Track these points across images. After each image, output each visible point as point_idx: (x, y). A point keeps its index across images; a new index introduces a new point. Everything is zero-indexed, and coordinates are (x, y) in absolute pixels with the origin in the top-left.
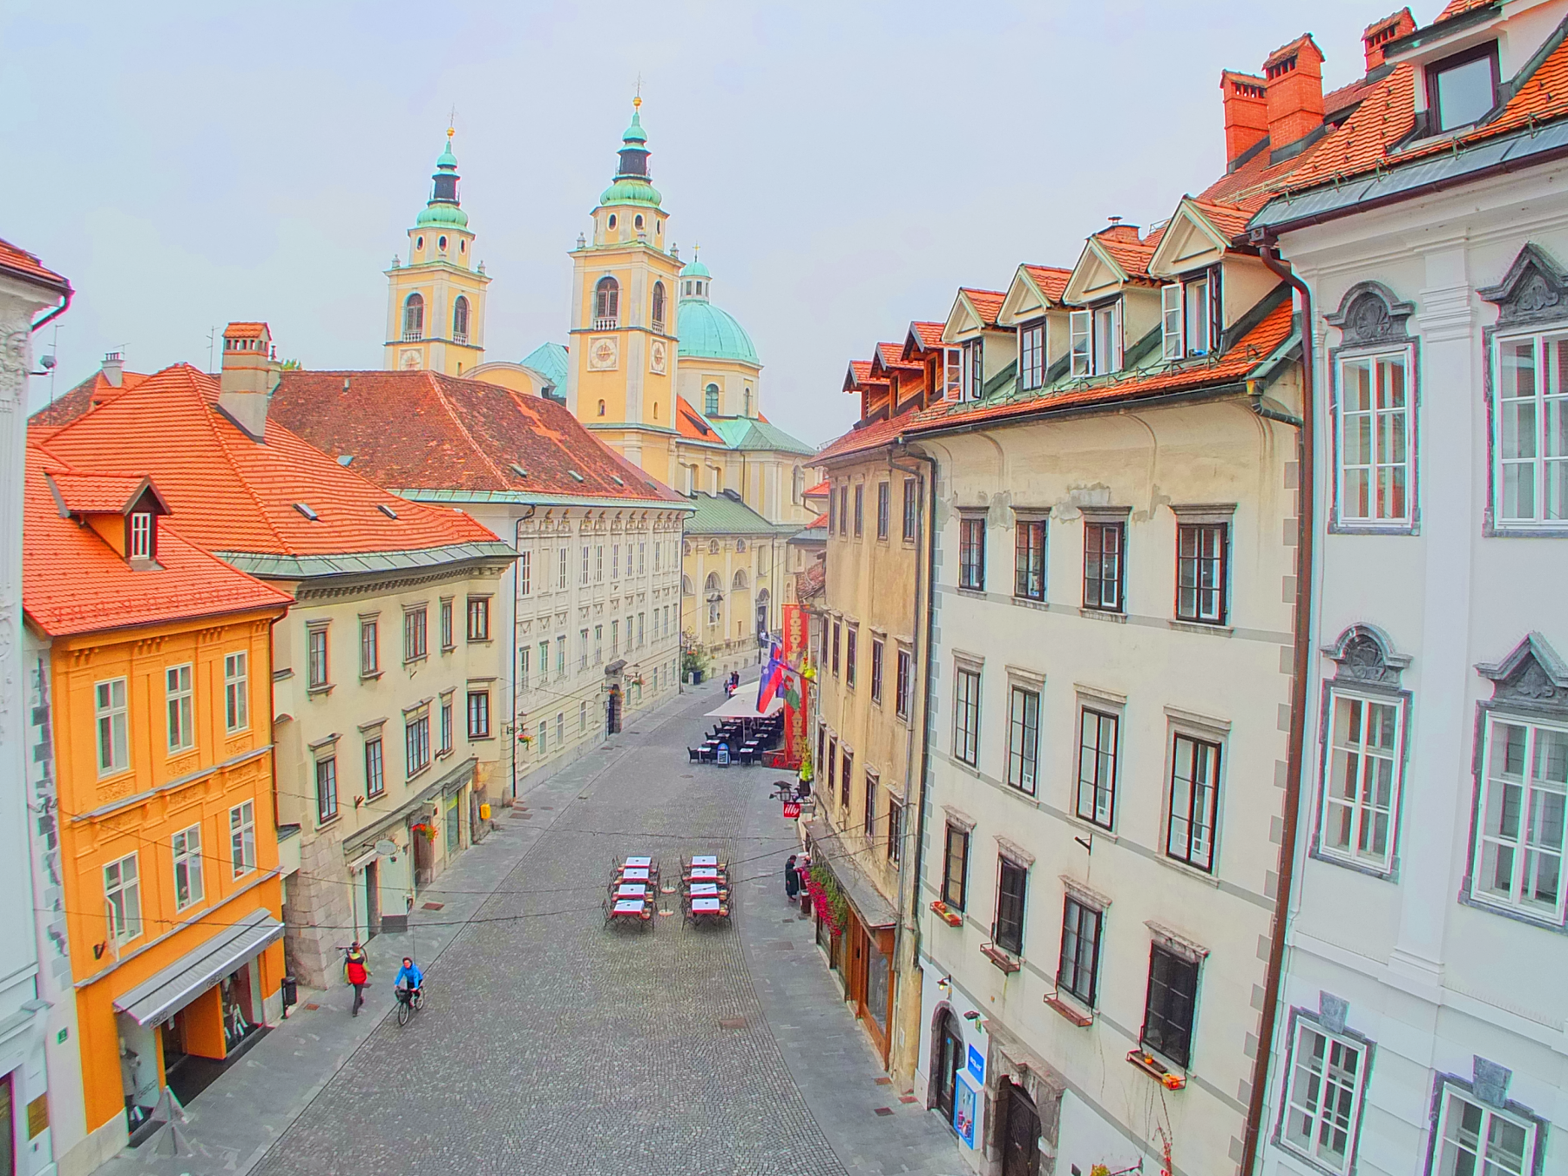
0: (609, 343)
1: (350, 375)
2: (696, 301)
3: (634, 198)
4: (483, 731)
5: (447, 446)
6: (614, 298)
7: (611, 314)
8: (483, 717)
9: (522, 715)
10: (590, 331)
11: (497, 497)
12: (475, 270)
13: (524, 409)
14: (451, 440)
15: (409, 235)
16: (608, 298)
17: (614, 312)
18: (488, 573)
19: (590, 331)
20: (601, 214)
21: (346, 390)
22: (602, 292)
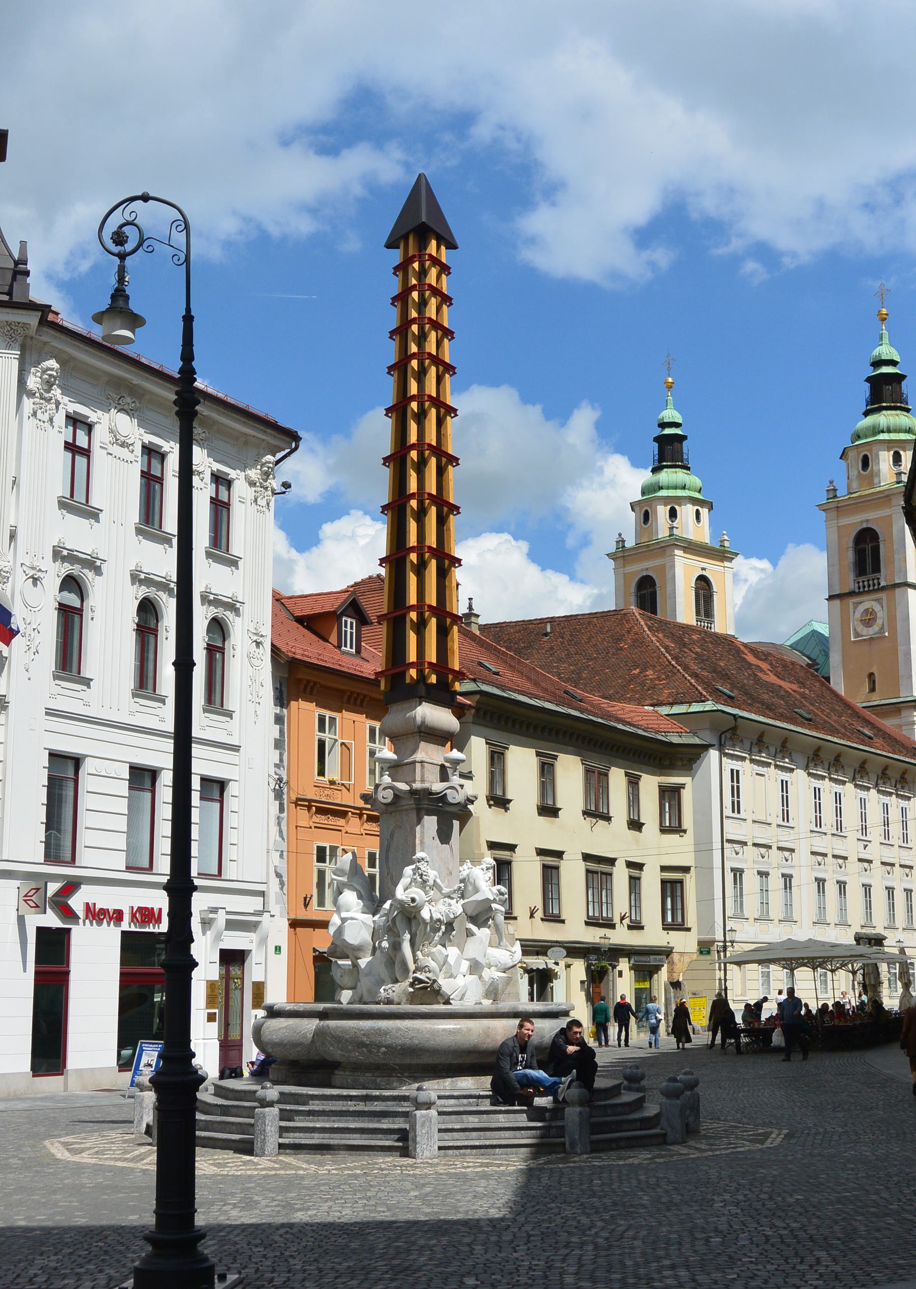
0: (877, 607)
1: (552, 620)
3: (889, 431)
5: (649, 672)
6: (876, 551)
7: (873, 572)
8: (679, 906)
9: (731, 930)
10: (852, 594)
11: (696, 707)
13: (750, 658)
14: (654, 667)
16: (869, 552)
17: (877, 568)
19: (852, 594)
20: (851, 454)
21: (546, 634)
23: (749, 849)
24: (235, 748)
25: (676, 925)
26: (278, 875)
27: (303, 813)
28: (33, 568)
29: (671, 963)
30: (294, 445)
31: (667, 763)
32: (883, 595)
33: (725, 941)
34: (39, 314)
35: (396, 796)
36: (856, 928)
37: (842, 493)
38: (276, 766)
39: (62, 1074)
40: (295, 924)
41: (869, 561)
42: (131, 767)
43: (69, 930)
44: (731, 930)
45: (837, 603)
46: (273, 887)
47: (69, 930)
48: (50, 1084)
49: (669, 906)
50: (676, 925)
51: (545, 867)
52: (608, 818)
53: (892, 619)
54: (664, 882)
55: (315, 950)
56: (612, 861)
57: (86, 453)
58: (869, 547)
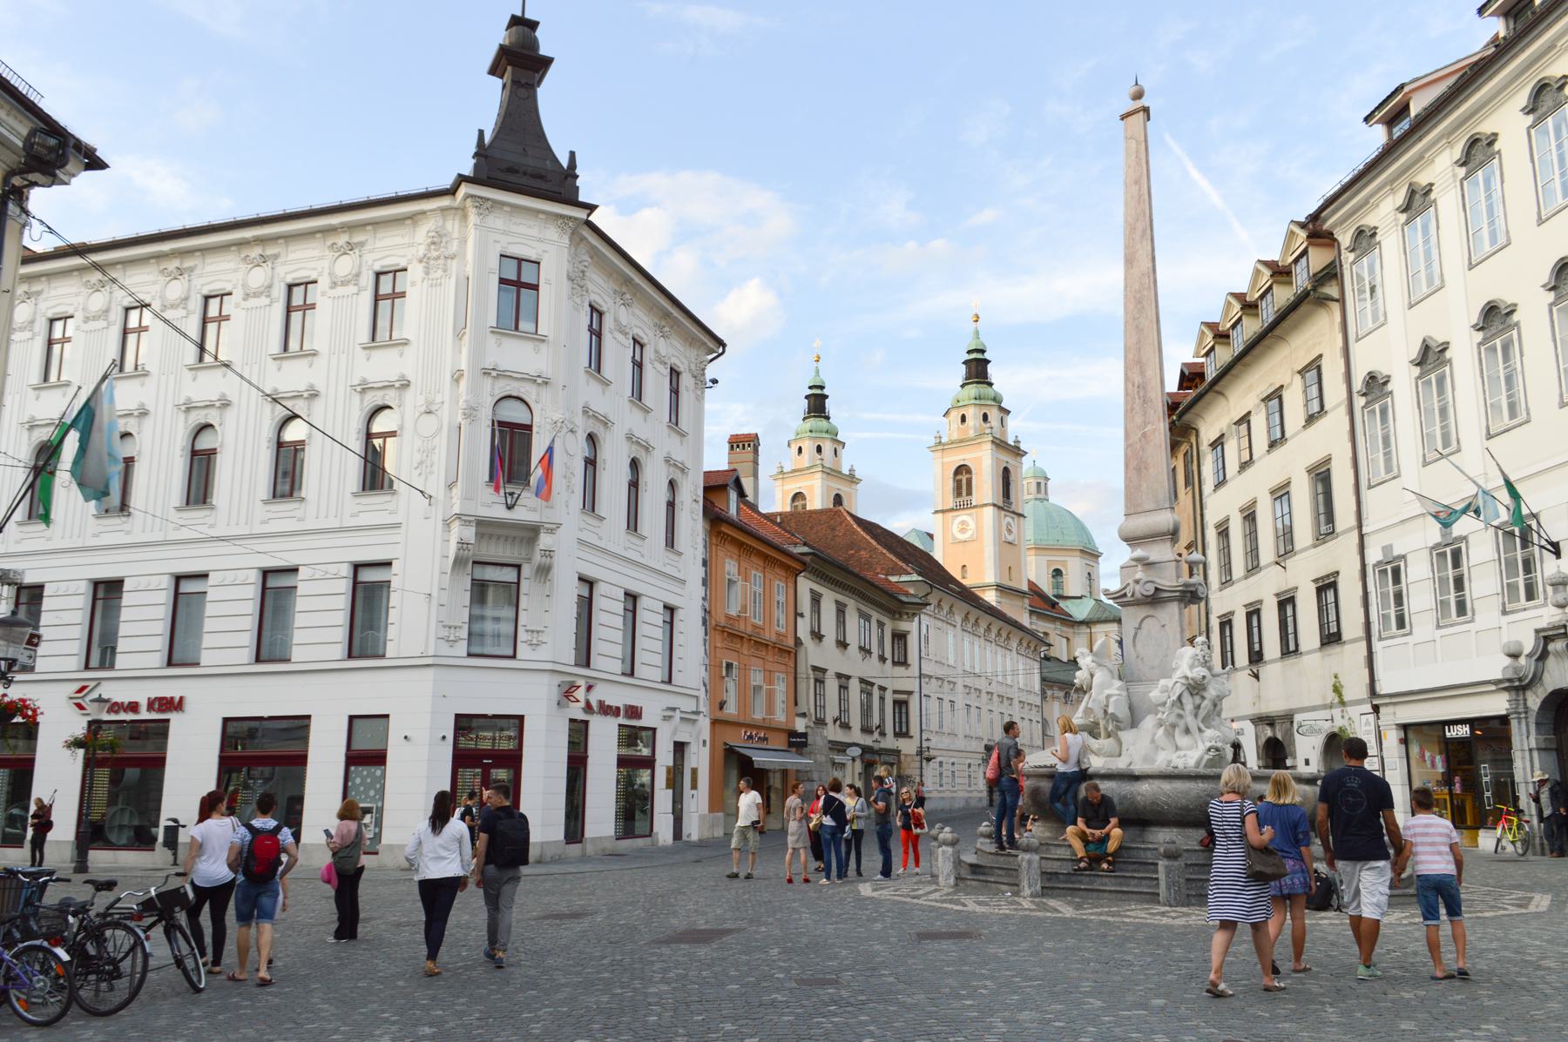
1: (781, 514)
2: (1036, 499)
3: (980, 399)
4: (904, 730)
5: (862, 553)
6: (969, 482)
9: (928, 740)
10: (952, 510)
11: (904, 578)
12: (847, 473)
15: (789, 445)
16: (964, 482)
17: (969, 493)
18: (905, 617)
19: (952, 510)
22: (959, 477)
23: (933, 680)
24: (683, 582)
25: (902, 733)
26: (705, 685)
27: (718, 637)
28: (572, 423)
29: (899, 762)
30: (721, 350)
31: (897, 616)
32: (973, 511)
33: (921, 747)
34: (588, 211)
35: (1157, 589)
36: (985, 742)
37: (944, 440)
38: (704, 599)
39: (581, 842)
40: (715, 723)
41: (964, 487)
42: (626, 594)
43: (586, 722)
44: (928, 740)
45: (940, 515)
46: (702, 694)
47: (586, 722)
48: (575, 849)
49: (897, 720)
50: (902, 733)
51: (840, 687)
52: (869, 652)
53: (979, 528)
54: (895, 702)
55: (726, 744)
56: (872, 684)
57: (599, 335)
58: (964, 478)
